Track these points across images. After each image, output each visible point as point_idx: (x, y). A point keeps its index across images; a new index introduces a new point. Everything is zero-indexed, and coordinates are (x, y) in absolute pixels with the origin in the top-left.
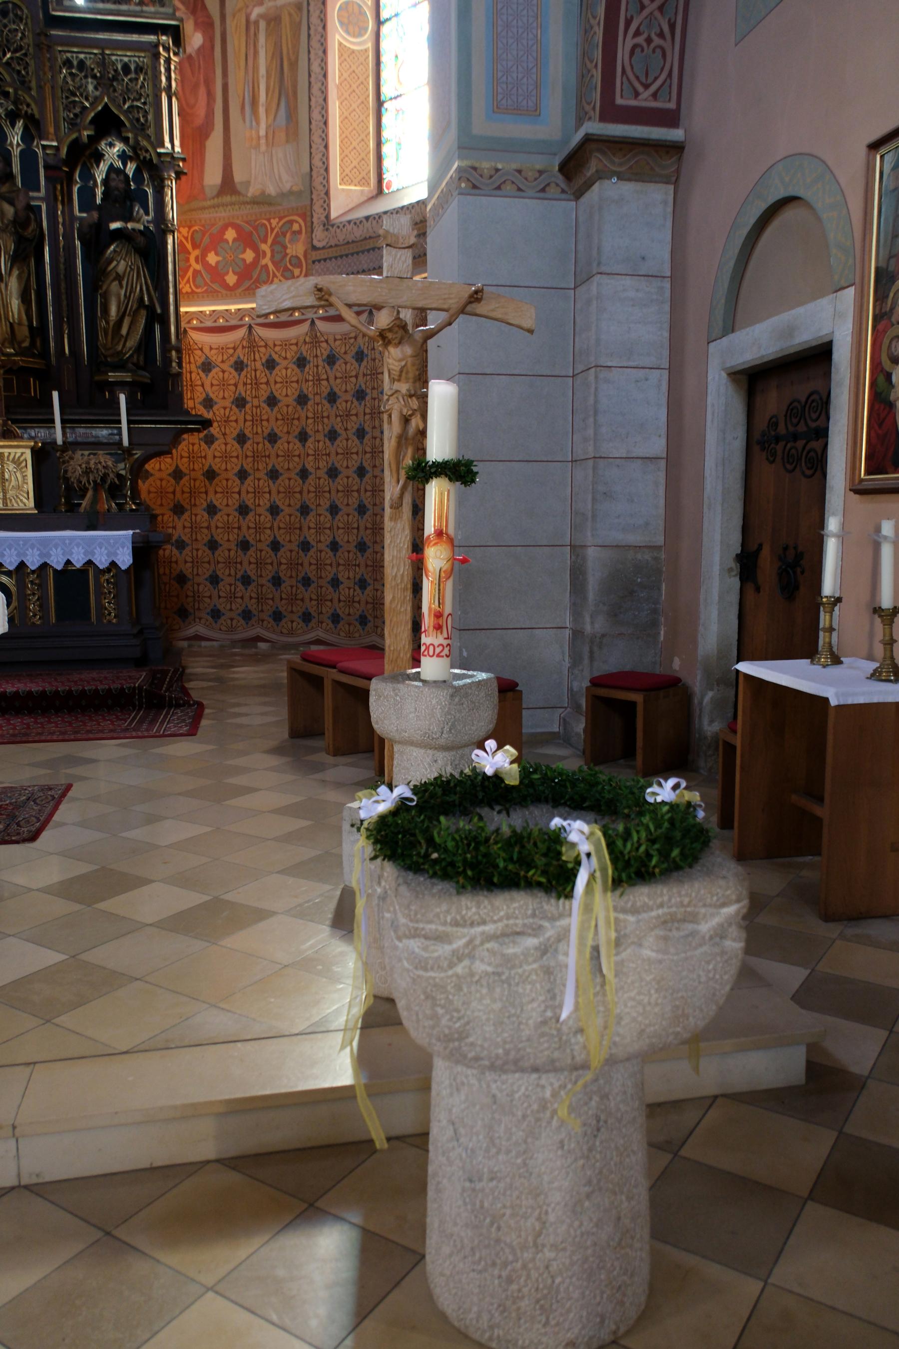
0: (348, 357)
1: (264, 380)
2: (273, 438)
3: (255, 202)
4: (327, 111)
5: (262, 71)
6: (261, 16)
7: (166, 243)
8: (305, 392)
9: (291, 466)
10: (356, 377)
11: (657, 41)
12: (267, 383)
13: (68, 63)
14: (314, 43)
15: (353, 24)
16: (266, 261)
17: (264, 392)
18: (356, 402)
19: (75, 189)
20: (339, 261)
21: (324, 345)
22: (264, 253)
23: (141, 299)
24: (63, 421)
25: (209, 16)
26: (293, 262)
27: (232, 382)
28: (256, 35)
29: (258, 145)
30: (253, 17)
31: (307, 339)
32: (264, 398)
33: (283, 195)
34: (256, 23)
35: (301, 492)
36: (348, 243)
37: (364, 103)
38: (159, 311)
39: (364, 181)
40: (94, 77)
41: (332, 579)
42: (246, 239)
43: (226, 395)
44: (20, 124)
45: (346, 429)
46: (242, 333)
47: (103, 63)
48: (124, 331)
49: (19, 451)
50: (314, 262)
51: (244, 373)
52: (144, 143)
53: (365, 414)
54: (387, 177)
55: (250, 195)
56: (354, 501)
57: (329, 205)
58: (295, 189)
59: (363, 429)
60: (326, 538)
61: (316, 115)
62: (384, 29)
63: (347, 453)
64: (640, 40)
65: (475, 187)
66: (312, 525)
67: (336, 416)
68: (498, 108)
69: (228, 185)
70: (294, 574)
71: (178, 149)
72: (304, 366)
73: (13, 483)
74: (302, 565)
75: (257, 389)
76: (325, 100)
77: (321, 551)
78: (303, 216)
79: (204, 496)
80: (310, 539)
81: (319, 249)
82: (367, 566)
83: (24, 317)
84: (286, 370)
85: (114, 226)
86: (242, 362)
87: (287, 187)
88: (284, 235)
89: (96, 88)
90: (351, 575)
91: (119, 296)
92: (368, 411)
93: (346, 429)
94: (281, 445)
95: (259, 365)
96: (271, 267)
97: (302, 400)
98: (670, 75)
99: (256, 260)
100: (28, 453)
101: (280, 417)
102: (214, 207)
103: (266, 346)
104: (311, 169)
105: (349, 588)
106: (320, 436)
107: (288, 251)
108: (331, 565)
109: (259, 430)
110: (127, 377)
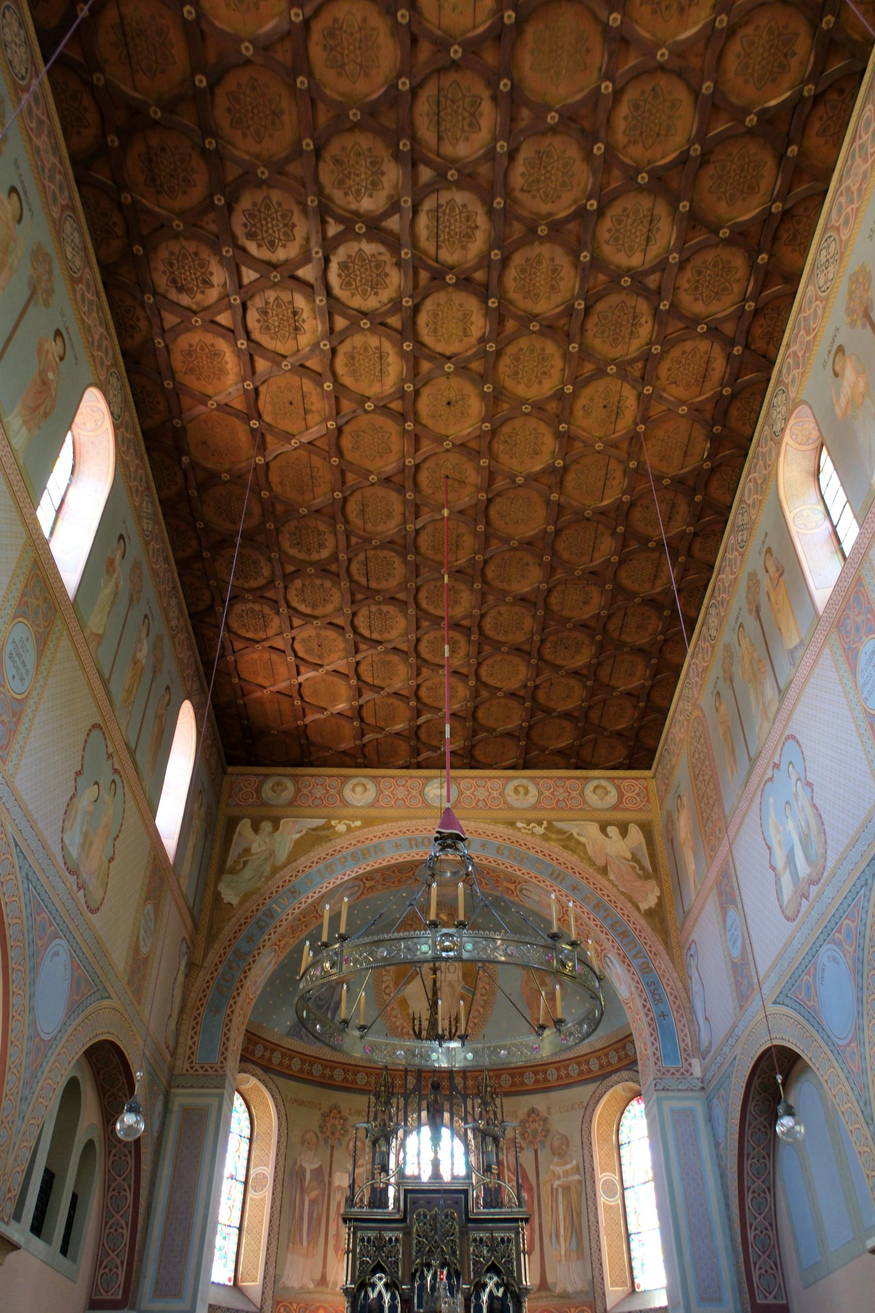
5: (561, 1216)
6: (559, 1186)
11: (770, 1271)
13: (475, 1240)
14: (590, 1203)
15: (610, 1192)
19: (472, 1305)
25: (531, 1185)
29: (561, 1260)
30: (555, 1186)
33: (577, 1293)
34: (557, 1189)
37: (620, 1235)
39: (623, 1284)
40: (487, 1246)
52: (512, 1281)
54: (637, 1281)
58: (584, 1289)
62: (627, 1193)
64: (763, 1271)
69: (543, 1284)
71: (528, 1284)
76: (598, 1236)
78: (590, 1307)
87: (579, 1287)
98: (780, 1287)
102: (536, 1298)
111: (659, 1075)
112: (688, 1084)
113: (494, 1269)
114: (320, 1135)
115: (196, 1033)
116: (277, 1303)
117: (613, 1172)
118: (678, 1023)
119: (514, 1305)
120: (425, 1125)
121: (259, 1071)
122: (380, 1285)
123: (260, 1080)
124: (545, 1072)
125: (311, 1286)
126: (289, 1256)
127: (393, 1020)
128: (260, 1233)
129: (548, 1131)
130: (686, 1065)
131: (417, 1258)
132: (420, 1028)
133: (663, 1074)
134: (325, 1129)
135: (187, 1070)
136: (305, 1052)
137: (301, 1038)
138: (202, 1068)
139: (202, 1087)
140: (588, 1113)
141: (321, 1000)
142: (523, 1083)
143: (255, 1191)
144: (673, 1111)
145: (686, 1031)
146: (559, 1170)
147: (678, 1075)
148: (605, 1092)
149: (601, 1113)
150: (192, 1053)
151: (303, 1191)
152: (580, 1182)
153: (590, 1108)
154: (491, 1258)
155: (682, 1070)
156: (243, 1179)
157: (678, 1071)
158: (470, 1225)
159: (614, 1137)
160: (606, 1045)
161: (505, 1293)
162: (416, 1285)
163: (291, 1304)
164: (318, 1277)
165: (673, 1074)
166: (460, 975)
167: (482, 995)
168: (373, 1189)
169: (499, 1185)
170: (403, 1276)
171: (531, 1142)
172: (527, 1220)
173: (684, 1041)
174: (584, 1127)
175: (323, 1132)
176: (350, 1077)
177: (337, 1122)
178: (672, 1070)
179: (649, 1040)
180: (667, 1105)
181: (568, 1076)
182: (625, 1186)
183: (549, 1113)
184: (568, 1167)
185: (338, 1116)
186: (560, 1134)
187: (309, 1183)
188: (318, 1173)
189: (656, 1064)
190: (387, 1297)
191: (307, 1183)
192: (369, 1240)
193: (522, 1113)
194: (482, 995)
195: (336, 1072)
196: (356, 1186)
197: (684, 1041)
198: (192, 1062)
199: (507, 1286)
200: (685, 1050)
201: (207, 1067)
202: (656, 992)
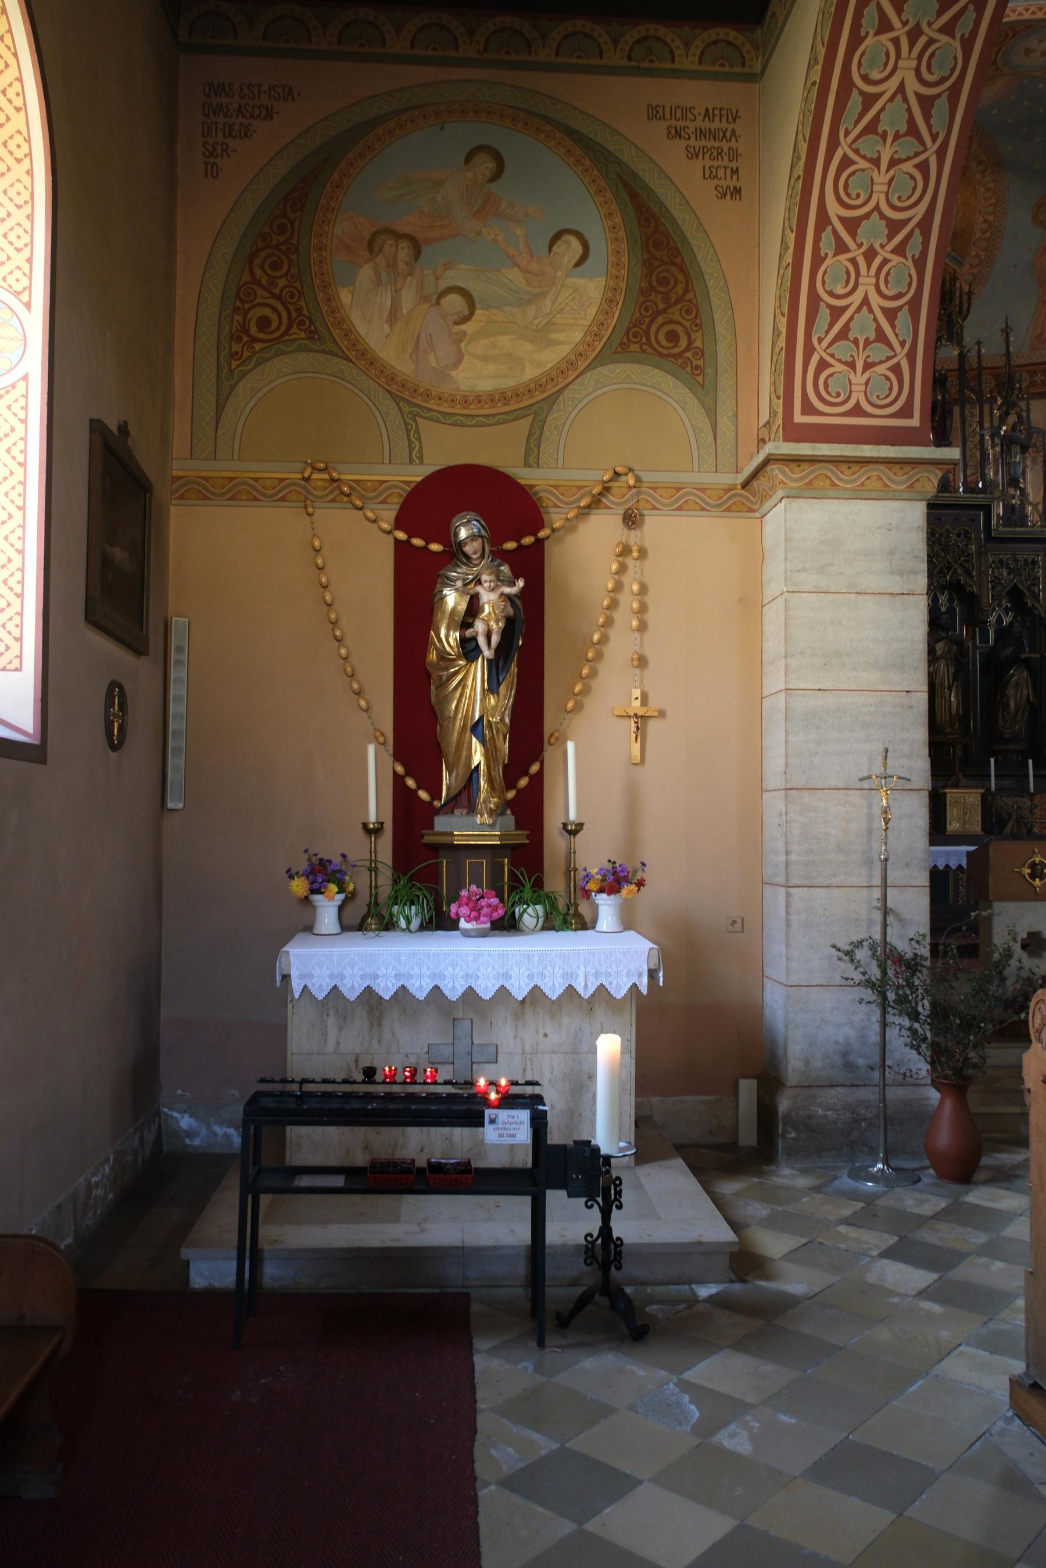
24: (996, 776)
47: (1016, 560)
52: (1036, 605)
89: (1009, 574)
100: (979, 796)
158: (989, 545)
167: (972, 266)
194: (972, 266)
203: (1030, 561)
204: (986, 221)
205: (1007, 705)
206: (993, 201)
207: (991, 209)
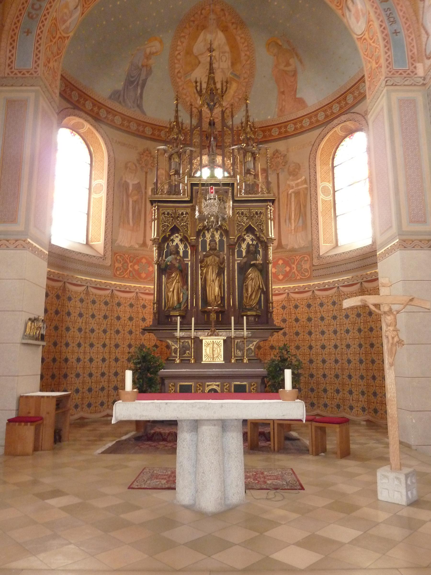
0: (329, 304)
1: (294, 312)
2: (297, 334)
3: (290, 251)
4: (318, 220)
5: (293, 209)
7: (269, 267)
8: (311, 316)
9: (305, 344)
10: (333, 311)
12: (295, 313)
14: (313, 199)
16: (294, 270)
17: (294, 317)
18: (333, 321)
20: (324, 270)
21: (318, 299)
22: (294, 268)
23: (259, 286)
26: (305, 270)
27: (281, 313)
28: (291, 198)
29: (291, 232)
30: (290, 192)
31: (311, 298)
32: (294, 319)
35: (309, 354)
36: (328, 263)
38: (265, 290)
39: (331, 242)
40: (247, 216)
41: (324, 389)
42: (286, 263)
43: (279, 318)
44: (219, 232)
45: (329, 331)
46: (285, 296)
47: (250, 212)
48: (253, 297)
49: (219, 340)
50: (313, 270)
51: (286, 310)
52: (262, 236)
53: (337, 325)
55: (288, 248)
56: (333, 358)
57: (319, 251)
59: (336, 331)
60: (321, 373)
61: (314, 222)
62: (336, 194)
63: (329, 340)
65: (405, 247)
66: (315, 367)
67: (324, 326)
68: (411, 222)
70: (307, 387)
72: (310, 307)
73: (216, 351)
74: (310, 383)
75: (291, 316)
76: (317, 217)
77: (318, 378)
78: (309, 255)
79: (269, 356)
80: (314, 373)
81: (315, 266)
82: (339, 384)
83: (220, 293)
84: (302, 309)
85: (252, 263)
86: (285, 306)
87: (303, 245)
88: (301, 261)
89: (247, 220)
90: (332, 388)
91: (252, 285)
92: (338, 323)
93: (329, 331)
94: (301, 336)
95: (291, 307)
96: (296, 272)
97: (309, 319)
99: (290, 271)
101: (300, 326)
103: (294, 300)
104: (312, 239)
105: (332, 393)
106: (318, 333)
107: (303, 267)
108: (323, 383)
109: (292, 331)
110: (254, 313)
111: (390, 74)
112: (412, 81)
113: (250, 230)
114: (138, 165)
115: (13, 48)
116: (114, 254)
117: (329, 182)
118: (407, 38)
119: (263, 250)
120: (206, 166)
121: (90, 118)
122: (177, 241)
123: (91, 125)
124: (286, 127)
125: (137, 246)
126: (121, 230)
127: (184, 97)
128: (100, 216)
129: (286, 162)
130: (412, 68)
131: (199, 223)
132: (201, 89)
133: (393, 74)
134: (141, 162)
135: (8, 74)
136: (123, 113)
137: (120, 103)
138: (20, 72)
139: (21, 86)
140: (314, 148)
141: (132, 77)
142: (271, 135)
143: (96, 193)
144: (400, 100)
145: (414, 43)
146: (293, 183)
147: (405, 75)
148: (328, 133)
149: (323, 147)
150: (12, 62)
151: (128, 196)
152: (306, 188)
153: (316, 144)
154: (248, 222)
155: (408, 72)
156: (88, 187)
157: (405, 72)
159: (331, 163)
160: (331, 101)
161: (257, 243)
162: (200, 240)
163: (124, 255)
164: (141, 242)
165: (401, 74)
166: (230, 64)
167: (245, 79)
168: (170, 186)
169: (255, 182)
170: (191, 234)
171: (275, 170)
172: (273, 201)
173: (411, 51)
174: (311, 156)
175: (140, 164)
176: (156, 133)
177: (149, 158)
178: (400, 72)
179: (382, 50)
180: (395, 96)
181: (302, 127)
182: (336, 190)
183: (288, 150)
184: (299, 181)
185: (149, 155)
186: (294, 163)
187: (132, 191)
188: (138, 187)
189: (388, 67)
190: (181, 248)
191: (130, 191)
192: (168, 214)
193: (270, 152)
194: (245, 79)
195: (147, 129)
196: (159, 182)
197: (411, 51)
198: (11, 68)
199: (258, 239)
200: (412, 58)
201: (24, 71)
202: (391, 16)
203: (259, 213)
204: (246, 55)
205: (247, 290)
206: (246, 44)
207: (246, 48)
